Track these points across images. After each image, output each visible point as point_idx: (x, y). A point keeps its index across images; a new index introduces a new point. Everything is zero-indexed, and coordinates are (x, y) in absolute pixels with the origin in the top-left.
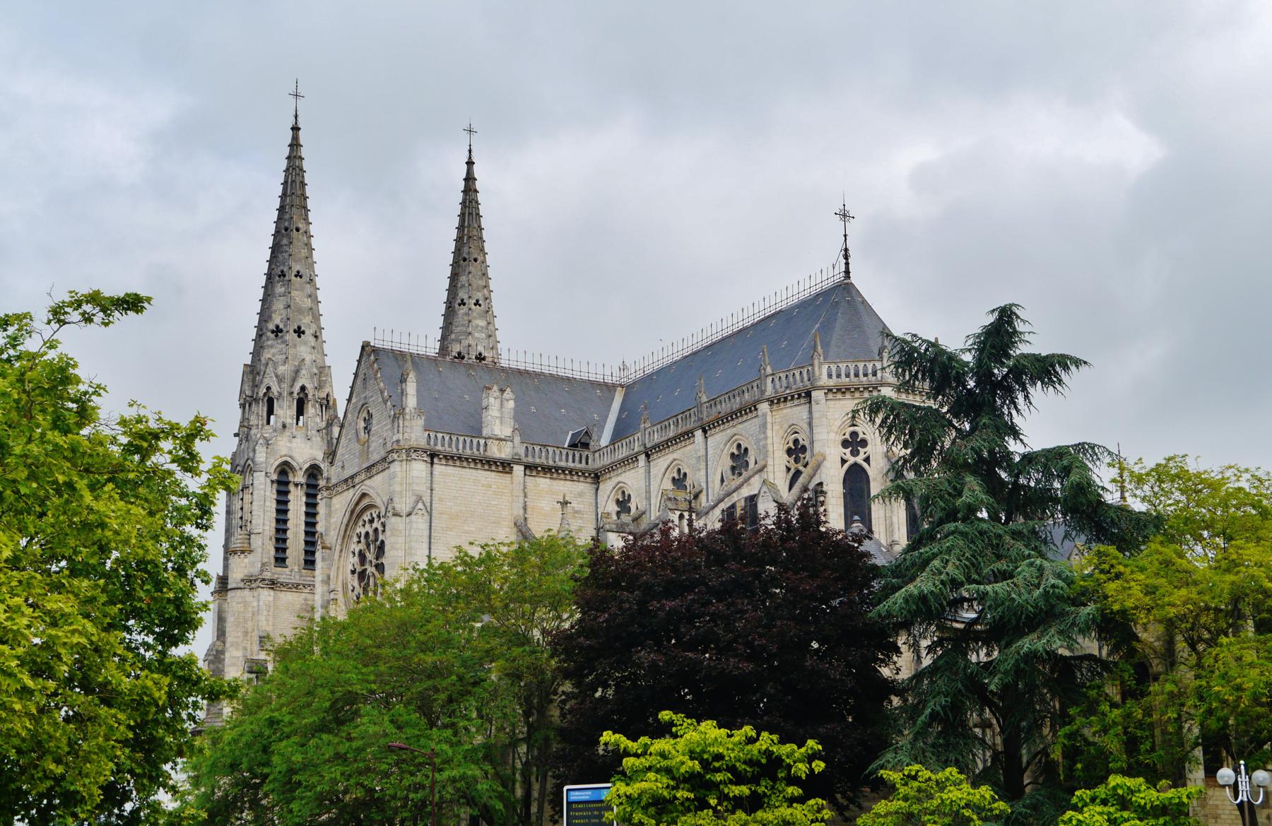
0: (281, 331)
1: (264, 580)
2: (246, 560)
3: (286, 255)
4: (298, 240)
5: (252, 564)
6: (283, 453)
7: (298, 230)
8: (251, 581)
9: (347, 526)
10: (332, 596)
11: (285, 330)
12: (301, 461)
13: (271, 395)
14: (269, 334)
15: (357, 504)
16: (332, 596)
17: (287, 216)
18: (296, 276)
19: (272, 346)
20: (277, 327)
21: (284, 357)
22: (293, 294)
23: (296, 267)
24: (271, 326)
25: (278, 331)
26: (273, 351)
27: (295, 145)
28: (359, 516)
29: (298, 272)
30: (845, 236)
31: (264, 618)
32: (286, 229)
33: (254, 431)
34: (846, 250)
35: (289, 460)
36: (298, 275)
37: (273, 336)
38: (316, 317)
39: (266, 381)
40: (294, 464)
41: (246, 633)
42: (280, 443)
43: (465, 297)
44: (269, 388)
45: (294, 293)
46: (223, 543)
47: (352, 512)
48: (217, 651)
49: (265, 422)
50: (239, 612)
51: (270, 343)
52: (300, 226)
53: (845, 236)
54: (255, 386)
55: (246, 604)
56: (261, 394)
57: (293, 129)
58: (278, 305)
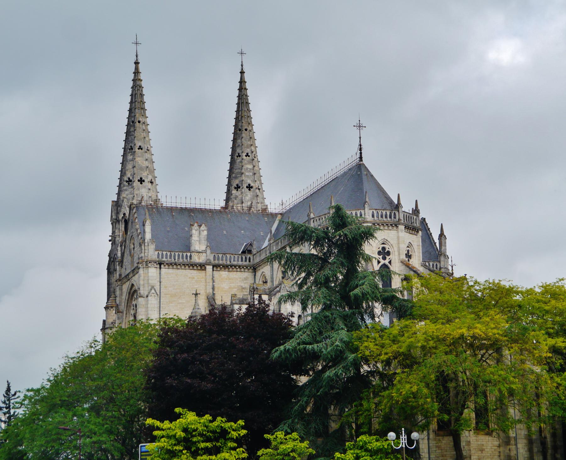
0: (131, 181)
3: (133, 137)
4: (140, 128)
7: (139, 122)
11: (133, 180)
14: (125, 183)
17: (133, 115)
18: (139, 149)
19: (126, 190)
20: (129, 179)
21: (132, 196)
22: (137, 160)
23: (138, 144)
24: (126, 179)
25: (129, 181)
26: (127, 192)
27: (137, 72)
29: (140, 146)
30: (360, 138)
34: (360, 145)
36: (140, 148)
37: (127, 184)
38: (152, 171)
43: (240, 152)
44: (124, 214)
45: (138, 159)
51: (125, 188)
52: (141, 119)
53: (360, 138)
54: (118, 213)
56: (120, 218)
57: (135, 63)
58: (129, 166)
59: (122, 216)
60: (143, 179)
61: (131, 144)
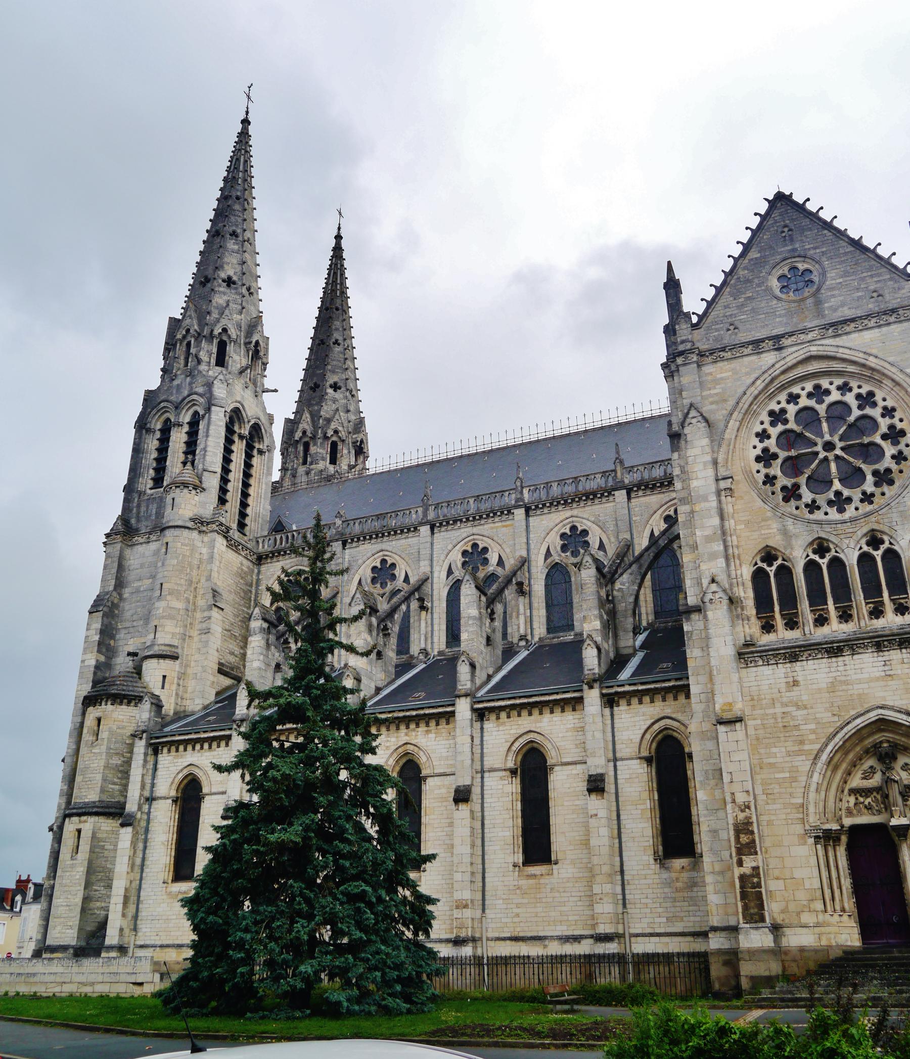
0: (234, 283)
1: (221, 524)
2: (196, 498)
5: (203, 504)
6: (239, 399)
8: (202, 523)
9: (756, 398)
10: (723, 484)
12: (249, 414)
13: (225, 338)
14: (220, 281)
15: (784, 372)
16: (723, 484)
17: (240, 188)
19: (224, 293)
20: (229, 278)
21: (240, 307)
24: (223, 275)
25: (229, 282)
26: (226, 298)
28: (782, 388)
31: (216, 569)
32: (238, 198)
33: (203, 367)
35: (241, 408)
37: (225, 284)
39: (224, 322)
40: (244, 415)
41: (190, 582)
42: (236, 387)
44: (225, 330)
46: (125, 482)
47: (772, 381)
48: (112, 603)
49: (213, 361)
50: (184, 556)
51: (221, 289)
55: (193, 549)
59: (220, 330)
60: (252, 290)
61: (234, 228)
